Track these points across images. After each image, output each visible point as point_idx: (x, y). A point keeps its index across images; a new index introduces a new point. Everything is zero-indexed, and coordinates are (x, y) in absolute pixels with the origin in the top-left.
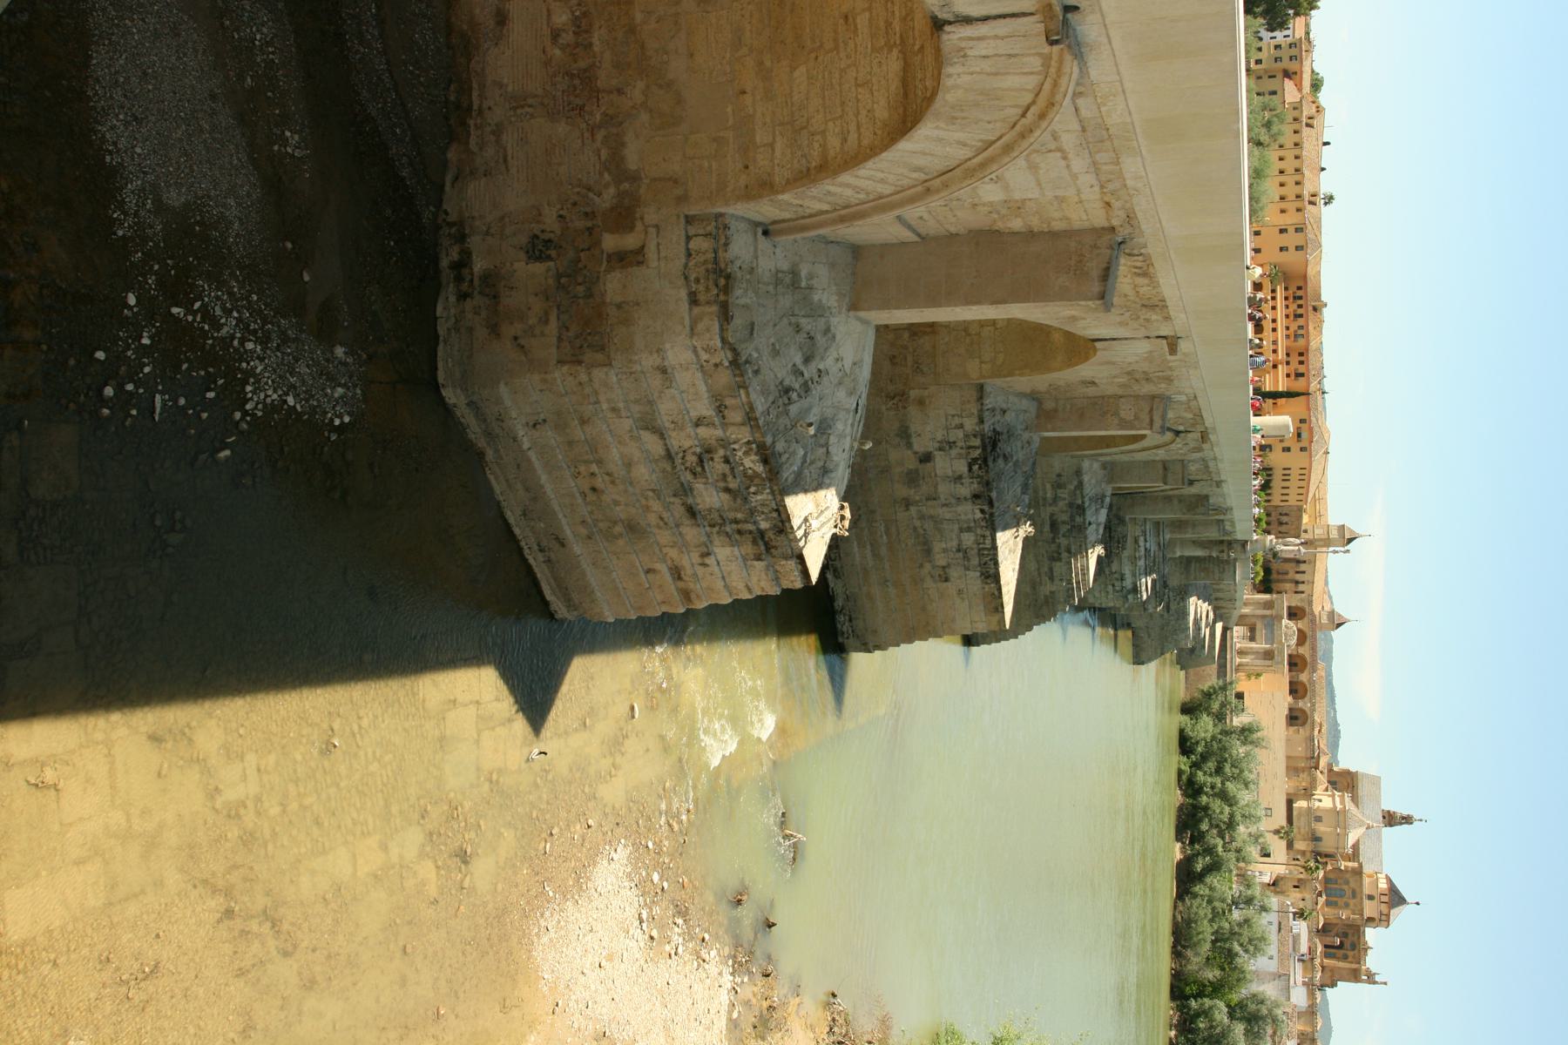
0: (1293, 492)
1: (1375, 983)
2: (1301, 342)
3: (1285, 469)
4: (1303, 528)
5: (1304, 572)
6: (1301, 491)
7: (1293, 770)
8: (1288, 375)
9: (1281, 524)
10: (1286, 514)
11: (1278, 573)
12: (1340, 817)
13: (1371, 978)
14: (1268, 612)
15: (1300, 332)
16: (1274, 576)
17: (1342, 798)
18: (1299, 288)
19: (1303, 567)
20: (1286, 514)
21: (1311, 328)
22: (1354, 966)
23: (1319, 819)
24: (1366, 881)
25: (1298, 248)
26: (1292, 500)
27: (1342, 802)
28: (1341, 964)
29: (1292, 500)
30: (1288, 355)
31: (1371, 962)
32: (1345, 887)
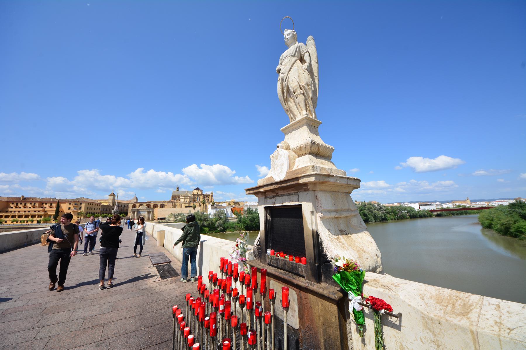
0: (96, 207)
3: (88, 209)
4: (108, 205)
5: (122, 205)
6: (96, 205)
7: (175, 206)
9: (107, 210)
10: (104, 209)
11: (121, 211)
14: (136, 213)
16: (122, 212)
19: (120, 205)
20: (104, 209)
22: (210, 196)
23: (186, 201)
24: (194, 194)
27: (183, 197)
28: (210, 198)
29: (99, 207)
31: (209, 193)
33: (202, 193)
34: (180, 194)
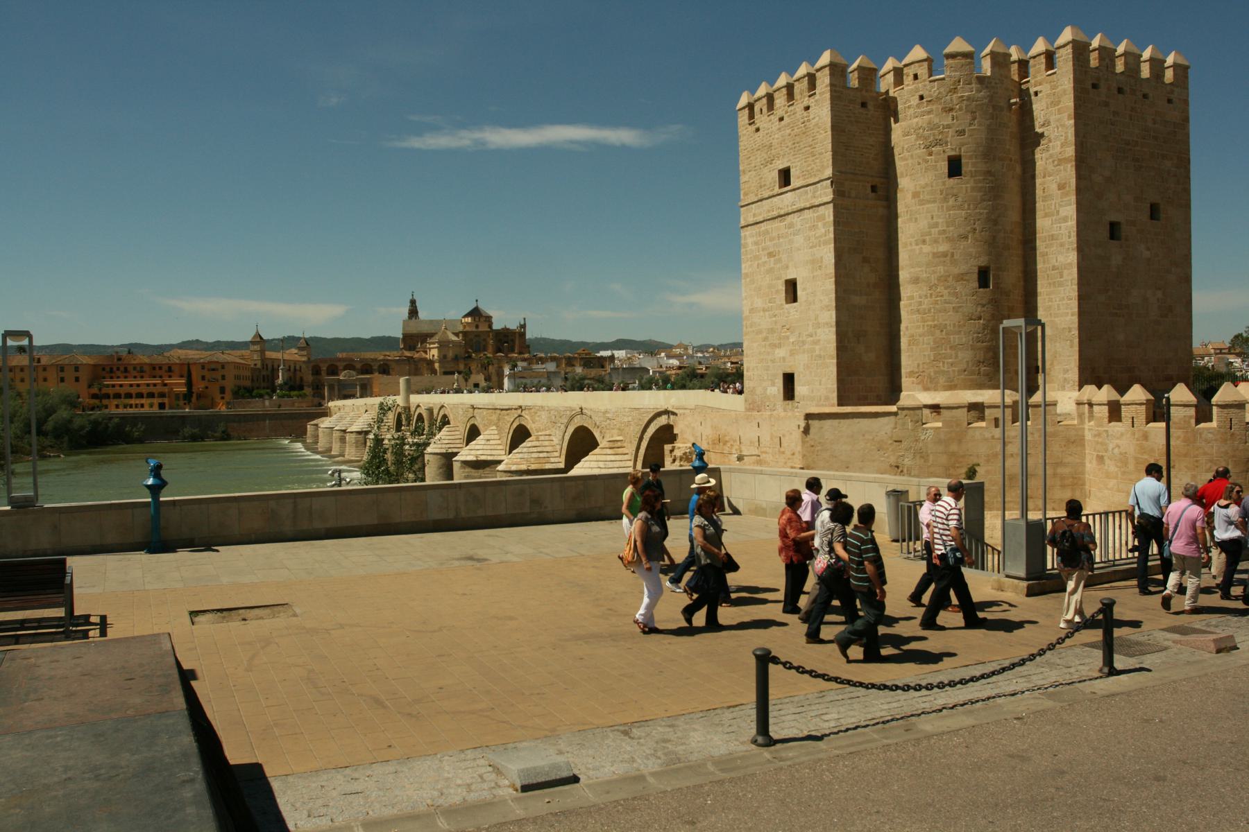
1: (525, 324)
2: (146, 368)
8: (170, 377)
12: (443, 345)
13: (523, 326)
14: (336, 388)
15: (138, 369)
17: (430, 343)
18: (104, 369)
21: (135, 362)
23: (445, 357)
24: (468, 329)
25: (77, 369)
26: (249, 374)
27: (434, 343)
28: (517, 342)
30: (155, 377)
31: (513, 326)
32: (474, 341)
33: (490, 326)
34: (425, 329)
